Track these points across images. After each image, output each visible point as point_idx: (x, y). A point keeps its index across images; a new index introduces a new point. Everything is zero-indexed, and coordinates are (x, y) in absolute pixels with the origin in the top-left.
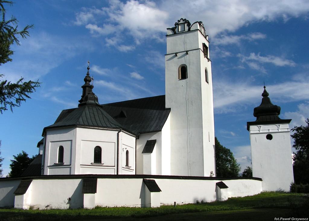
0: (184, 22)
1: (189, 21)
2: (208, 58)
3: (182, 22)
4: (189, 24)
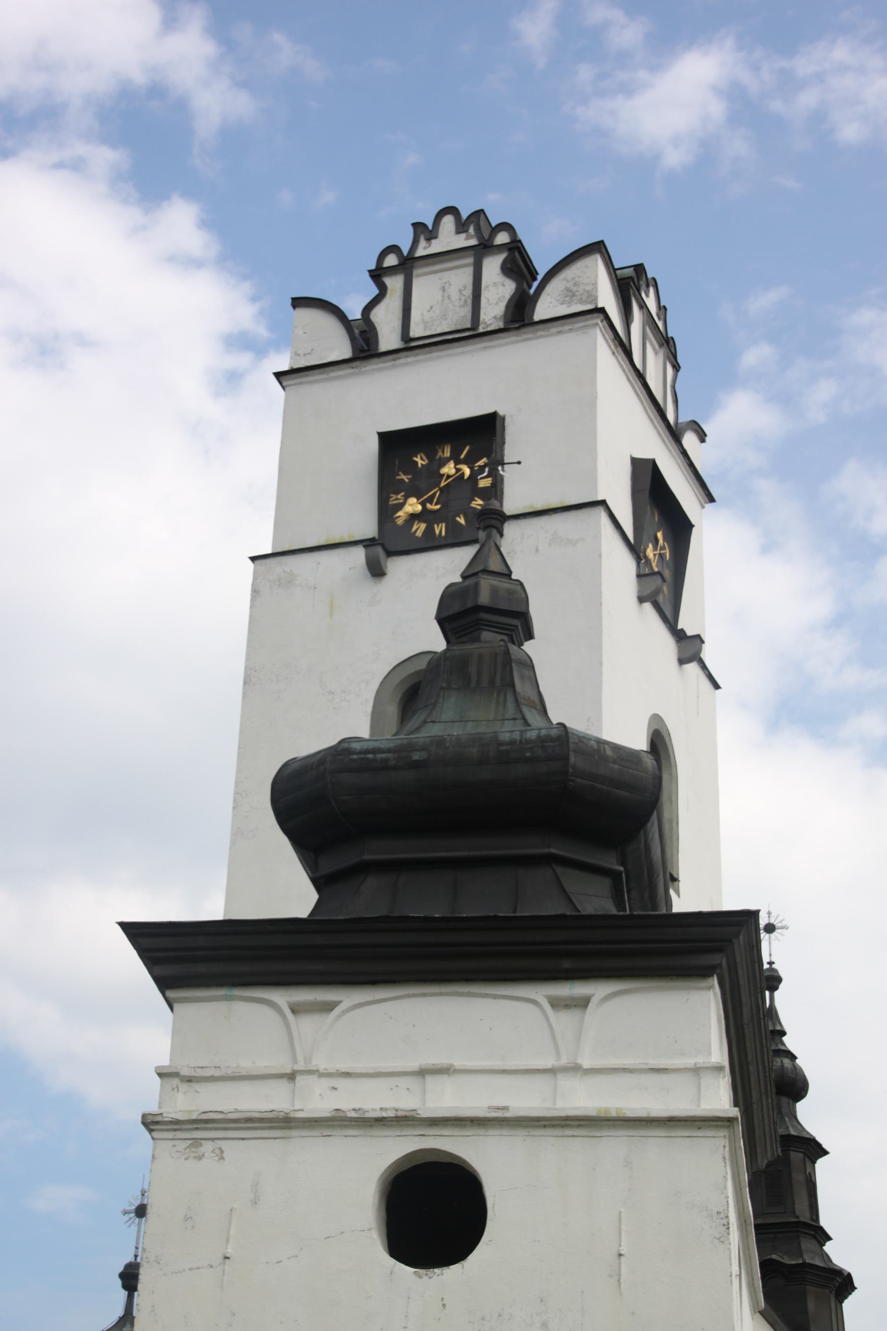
1: (522, 235)
2: (679, 636)
3: (449, 238)
4: (518, 264)
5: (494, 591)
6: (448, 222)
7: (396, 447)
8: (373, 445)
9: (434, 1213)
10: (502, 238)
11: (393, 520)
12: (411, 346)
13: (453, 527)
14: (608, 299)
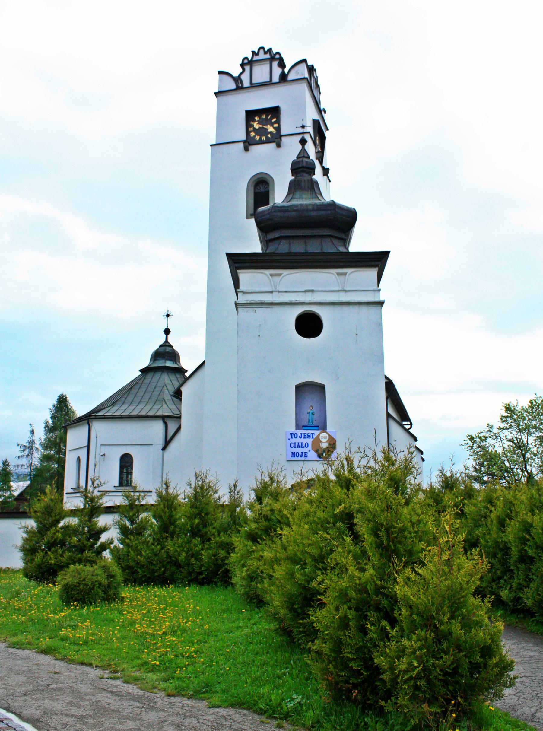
0: (268, 56)
1: (282, 56)
3: (262, 56)
4: (282, 65)
5: (307, 162)
6: (262, 51)
7: (250, 115)
8: (244, 114)
9: (309, 325)
10: (277, 56)
11: (250, 135)
12: (253, 86)
13: (267, 137)
14: (307, 75)
